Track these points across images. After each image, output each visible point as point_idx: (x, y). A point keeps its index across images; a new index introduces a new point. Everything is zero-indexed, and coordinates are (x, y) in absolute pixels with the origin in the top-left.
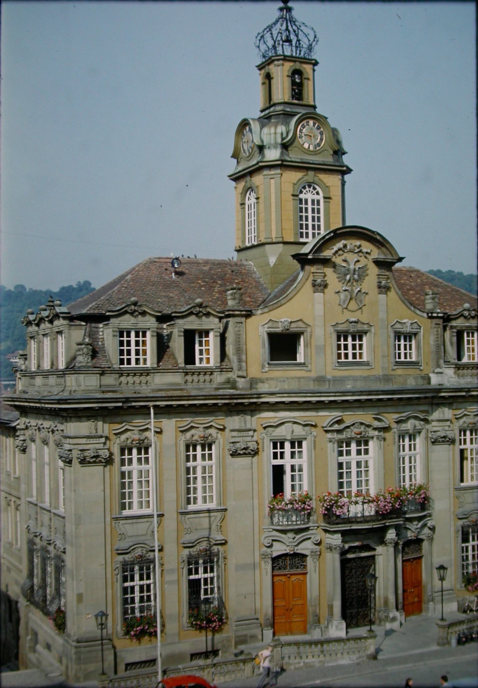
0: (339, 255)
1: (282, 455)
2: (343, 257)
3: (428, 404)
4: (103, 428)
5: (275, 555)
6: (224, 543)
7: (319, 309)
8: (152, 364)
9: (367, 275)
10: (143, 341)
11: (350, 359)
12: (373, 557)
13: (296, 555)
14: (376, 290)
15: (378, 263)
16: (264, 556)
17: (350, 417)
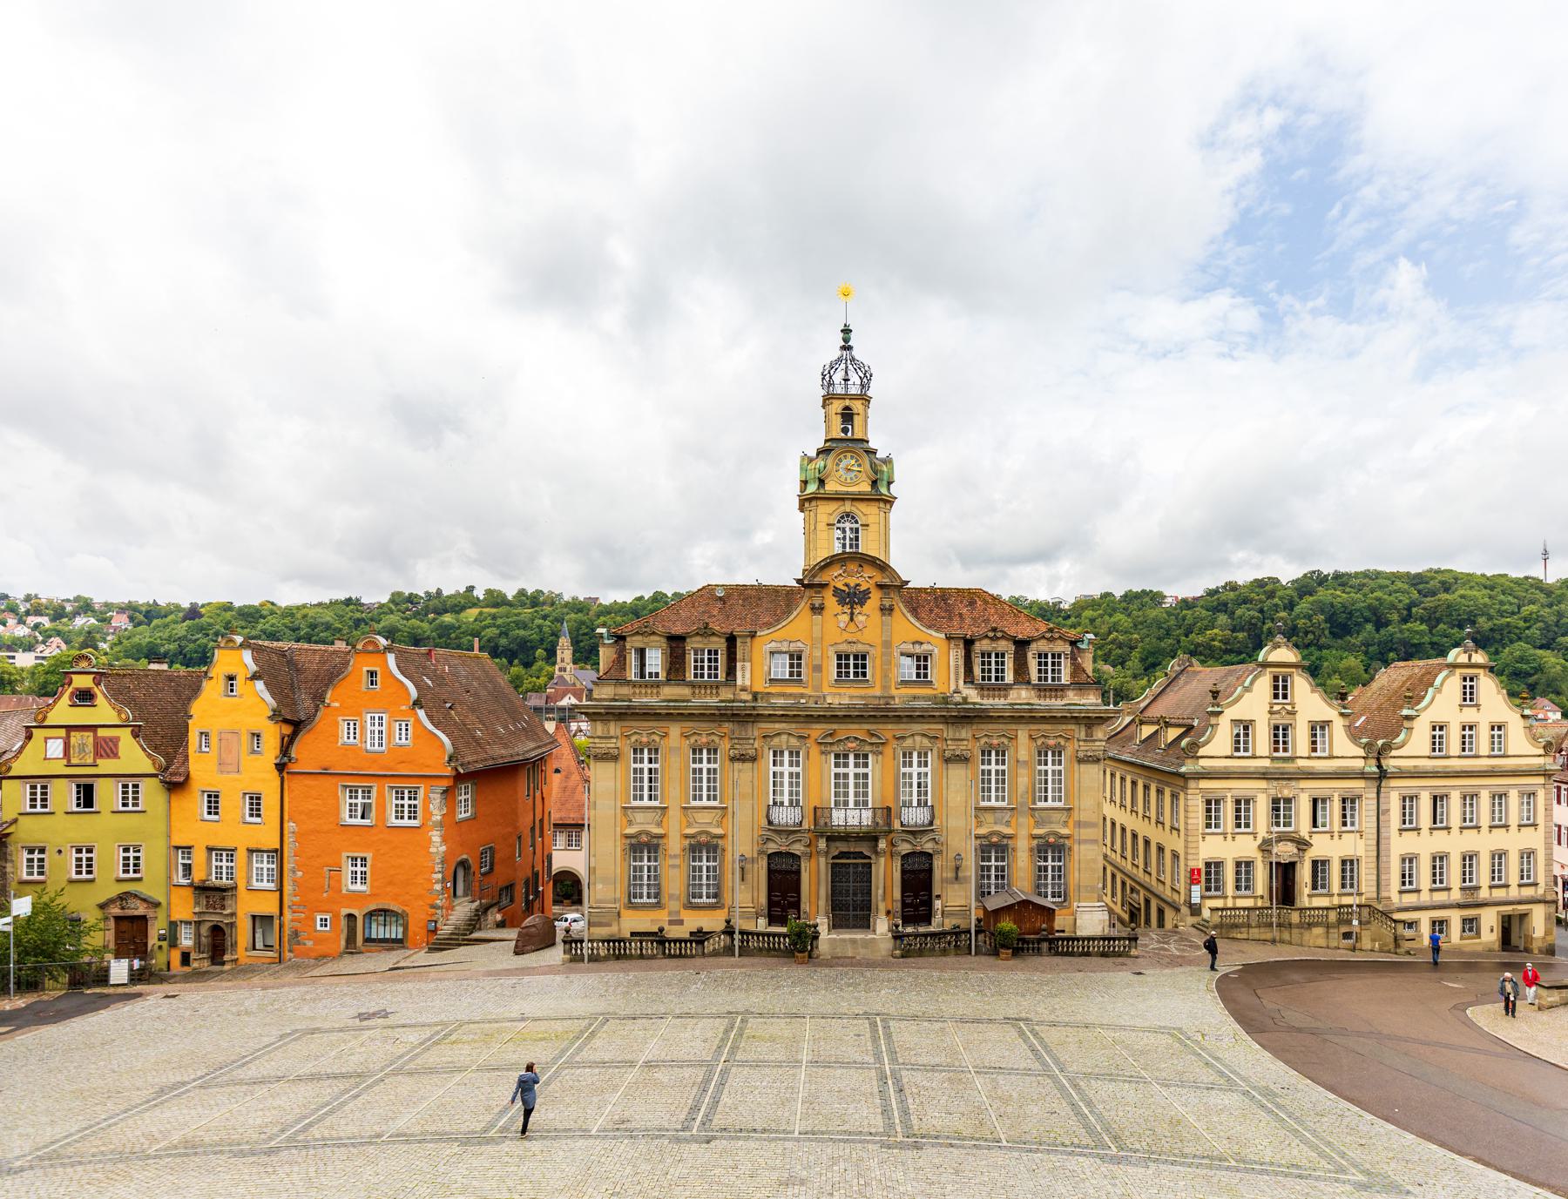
4: (614, 728)
6: (721, 837)
12: (870, 865)
15: (880, 587)
16: (761, 853)
17: (844, 730)
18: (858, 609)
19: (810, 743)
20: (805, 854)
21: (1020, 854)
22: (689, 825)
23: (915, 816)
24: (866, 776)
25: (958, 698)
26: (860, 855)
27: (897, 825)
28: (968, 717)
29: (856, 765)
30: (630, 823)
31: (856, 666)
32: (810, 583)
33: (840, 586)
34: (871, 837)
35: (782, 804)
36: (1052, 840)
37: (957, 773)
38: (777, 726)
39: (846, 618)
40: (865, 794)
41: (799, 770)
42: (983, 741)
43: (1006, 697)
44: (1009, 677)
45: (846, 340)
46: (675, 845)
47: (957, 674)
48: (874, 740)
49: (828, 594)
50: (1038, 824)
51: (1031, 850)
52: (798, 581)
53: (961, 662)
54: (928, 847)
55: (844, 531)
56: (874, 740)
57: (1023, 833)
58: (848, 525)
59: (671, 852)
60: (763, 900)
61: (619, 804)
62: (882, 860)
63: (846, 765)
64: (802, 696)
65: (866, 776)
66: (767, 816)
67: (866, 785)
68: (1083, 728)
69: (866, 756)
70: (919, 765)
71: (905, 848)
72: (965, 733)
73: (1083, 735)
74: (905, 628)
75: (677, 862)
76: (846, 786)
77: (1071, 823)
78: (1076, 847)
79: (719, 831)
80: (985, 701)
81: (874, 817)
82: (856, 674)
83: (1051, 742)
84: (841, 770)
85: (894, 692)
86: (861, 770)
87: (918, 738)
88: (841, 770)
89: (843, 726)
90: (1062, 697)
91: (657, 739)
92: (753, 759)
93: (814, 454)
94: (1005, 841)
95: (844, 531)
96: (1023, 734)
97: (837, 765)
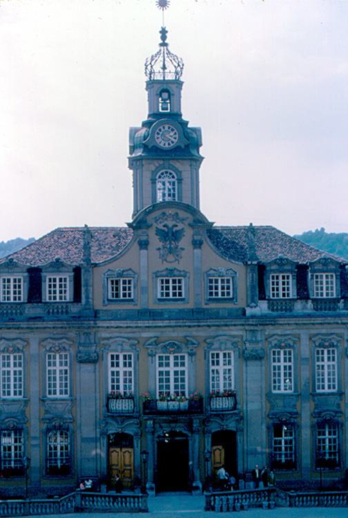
0: (160, 223)
1: (118, 365)
2: (163, 224)
7: (144, 262)
8: (70, 299)
9: (184, 236)
10: (163, 283)
11: (220, 296)
14: (192, 246)
16: (102, 434)
20: (136, 434)
24: (183, 373)
29: (176, 365)
31: (174, 288)
32: (139, 224)
33: (161, 226)
37: (254, 368)
40: (183, 387)
41: (48, 368)
44: (293, 293)
45: (164, 37)
49: (152, 232)
51: (312, 427)
52: (128, 224)
54: (231, 425)
55: (164, 184)
58: (166, 180)
59: (32, 434)
63: (168, 365)
65: (183, 373)
66: (107, 405)
67: (183, 380)
69: (183, 358)
71: (214, 427)
74: (210, 258)
76: (168, 380)
82: (174, 294)
84: (164, 369)
86: (179, 369)
88: (164, 369)
92: (94, 362)
93: (140, 125)
95: (164, 184)
97: (161, 365)
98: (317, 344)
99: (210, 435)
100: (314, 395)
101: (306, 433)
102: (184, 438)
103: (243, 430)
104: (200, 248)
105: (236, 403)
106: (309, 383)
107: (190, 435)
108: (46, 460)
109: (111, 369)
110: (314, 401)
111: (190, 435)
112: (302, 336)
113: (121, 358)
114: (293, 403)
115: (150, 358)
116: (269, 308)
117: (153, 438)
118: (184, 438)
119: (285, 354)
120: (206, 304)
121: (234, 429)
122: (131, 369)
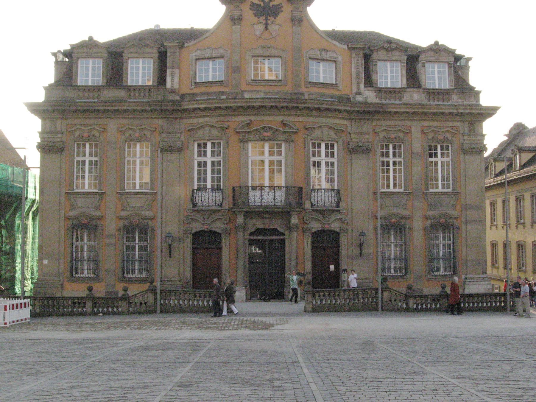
3: (346, 119)
5: (194, 231)
6: (152, 219)
9: (282, 11)
12: (283, 241)
13: (211, 232)
16: (186, 232)
18: (271, 19)
19: (230, 132)
21: (415, 233)
22: (123, 209)
23: (323, 199)
25: (359, 98)
26: (275, 232)
27: (307, 205)
28: (367, 113)
30: (73, 207)
34: (284, 213)
35: (205, 188)
36: (442, 220)
37: (360, 163)
38: (201, 120)
39: (261, 27)
42: (382, 135)
43: (401, 99)
46: (111, 225)
47: (358, 78)
48: (287, 130)
50: (431, 207)
53: (362, 70)
54: (335, 226)
56: (287, 130)
57: (418, 214)
60: (188, 274)
61: (63, 191)
62: (295, 234)
64: (223, 93)
68: (467, 125)
70: (327, 155)
71: (315, 226)
72: (367, 127)
73: (467, 130)
75: (113, 241)
77: (458, 208)
78: (463, 227)
79: (149, 214)
80: (383, 102)
81: (287, 195)
83: (441, 137)
85: (303, 90)
86: (275, 158)
87: (325, 131)
89: (259, 118)
90: (449, 100)
91: (97, 134)
92: (180, 150)
94: (403, 221)
96: (416, 128)
98: (430, 137)
99: (310, 235)
100: (426, 195)
101: (418, 237)
102: (282, 237)
103: (347, 231)
104: (300, 25)
105: (339, 201)
106: (421, 179)
107: (287, 233)
108: (123, 261)
109: (197, 159)
110: (426, 200)
111: (287, 233)
112: (413, 129)
113: (209, 146)
114: (404, 202)
115: (242, 144)
116: (376, 96)
117: (244, 235)
118: (282, 237)
119: (394, 148)
120: (306, 87)
121: (338, 230)
122: (220, 159)
